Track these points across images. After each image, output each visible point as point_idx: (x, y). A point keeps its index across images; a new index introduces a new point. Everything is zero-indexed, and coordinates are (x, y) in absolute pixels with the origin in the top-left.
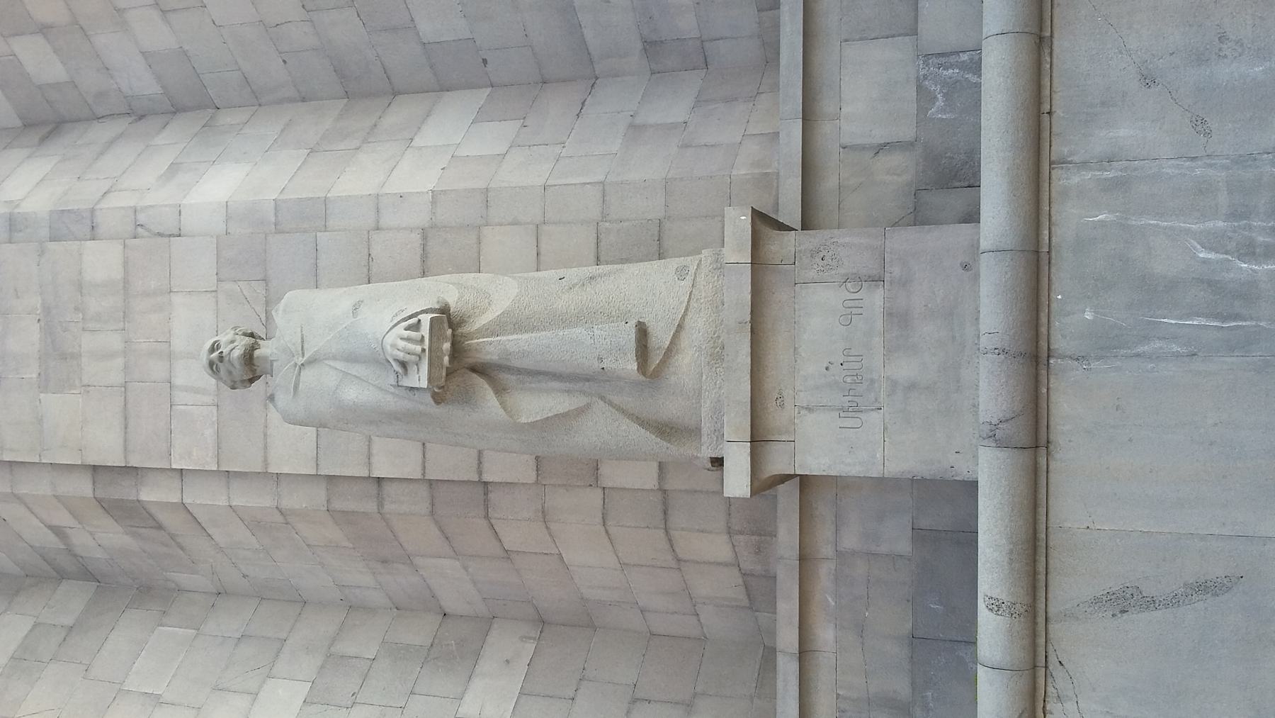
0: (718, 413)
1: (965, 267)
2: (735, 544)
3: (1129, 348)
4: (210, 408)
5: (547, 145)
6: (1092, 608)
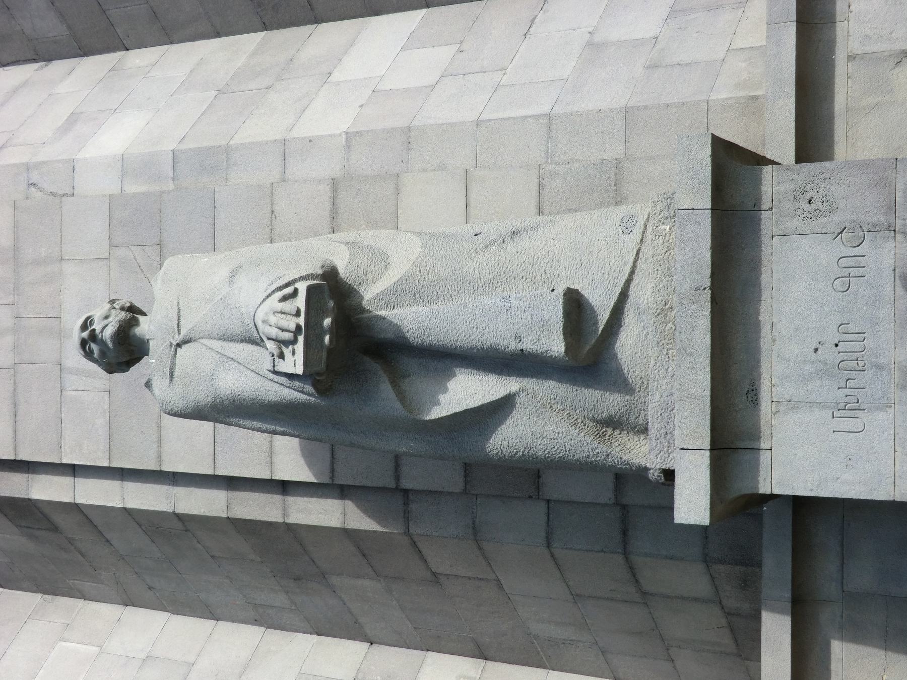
0: (668, 409)
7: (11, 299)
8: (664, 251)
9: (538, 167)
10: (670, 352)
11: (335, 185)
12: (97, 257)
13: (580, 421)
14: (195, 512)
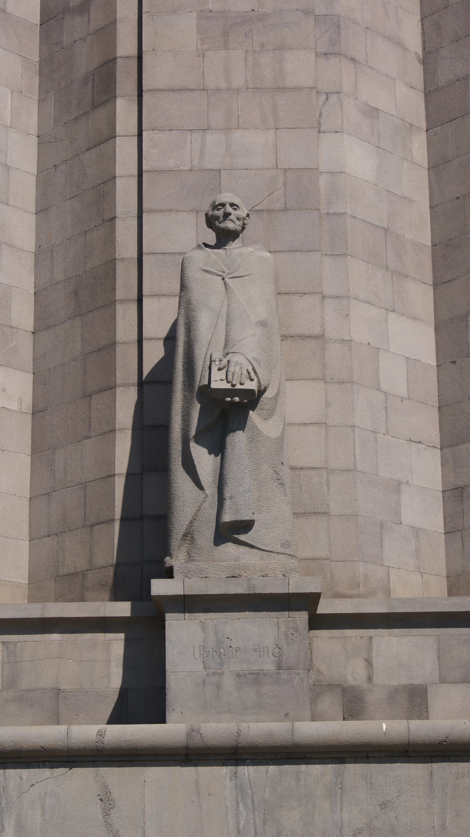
1: (287, 715)
2: (107, 568)
5: (386, 421)
6: (102, 784)
7: (251, 86)
8: (271, 568)
9: (326, 467)
10: (226, 572)
11: (320, 337)
12: (278, 158)
13: (192, 524)
14: (117, 234)
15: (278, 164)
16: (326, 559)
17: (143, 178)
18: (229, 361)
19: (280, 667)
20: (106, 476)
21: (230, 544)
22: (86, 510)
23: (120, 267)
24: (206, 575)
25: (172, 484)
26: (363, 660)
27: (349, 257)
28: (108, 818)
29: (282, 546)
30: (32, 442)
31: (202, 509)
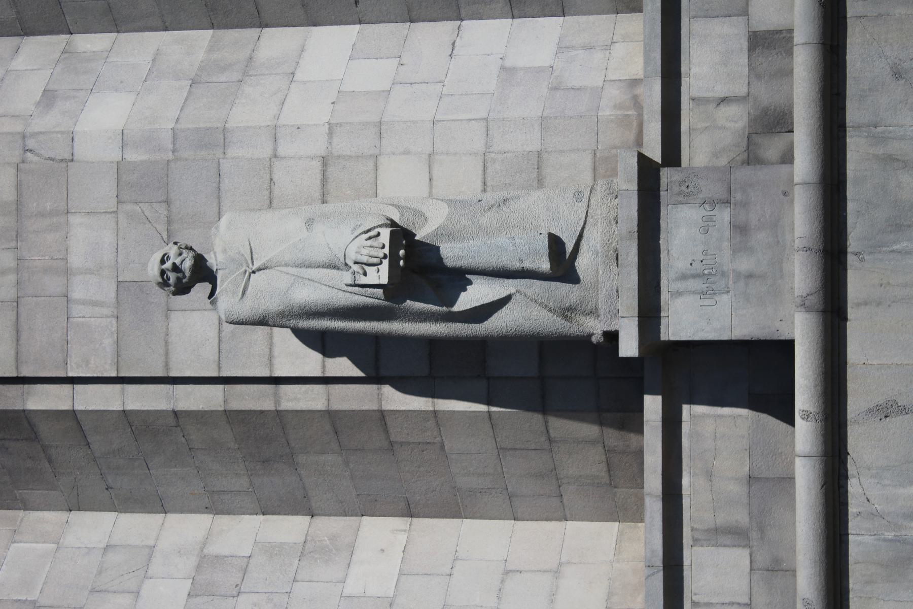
1: (785, 194)
3: (888, 246)
4: (109, 320)
7: (13, 244)
8: (607, 212)
10: (611, 267)
11: (325, 161)
12: (104, 211)
13: (552, 309)
15: (111, 210)
16: (595, 154)
17: (126, 375)
18: (356, 263)
19: (727, 201)
20: (490, 423)
21: (577, 264)
22: (530, 448)
23: (235, 405)
24: (615, 291)
25: (504, 333)
26: (718, 108)
27: (227, 125)
28: (909, 409)
29: (579, 200)
30: (446, 518)
31: (534, 297)
